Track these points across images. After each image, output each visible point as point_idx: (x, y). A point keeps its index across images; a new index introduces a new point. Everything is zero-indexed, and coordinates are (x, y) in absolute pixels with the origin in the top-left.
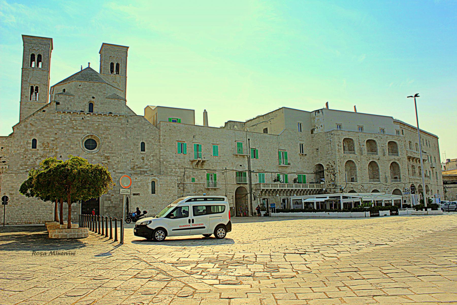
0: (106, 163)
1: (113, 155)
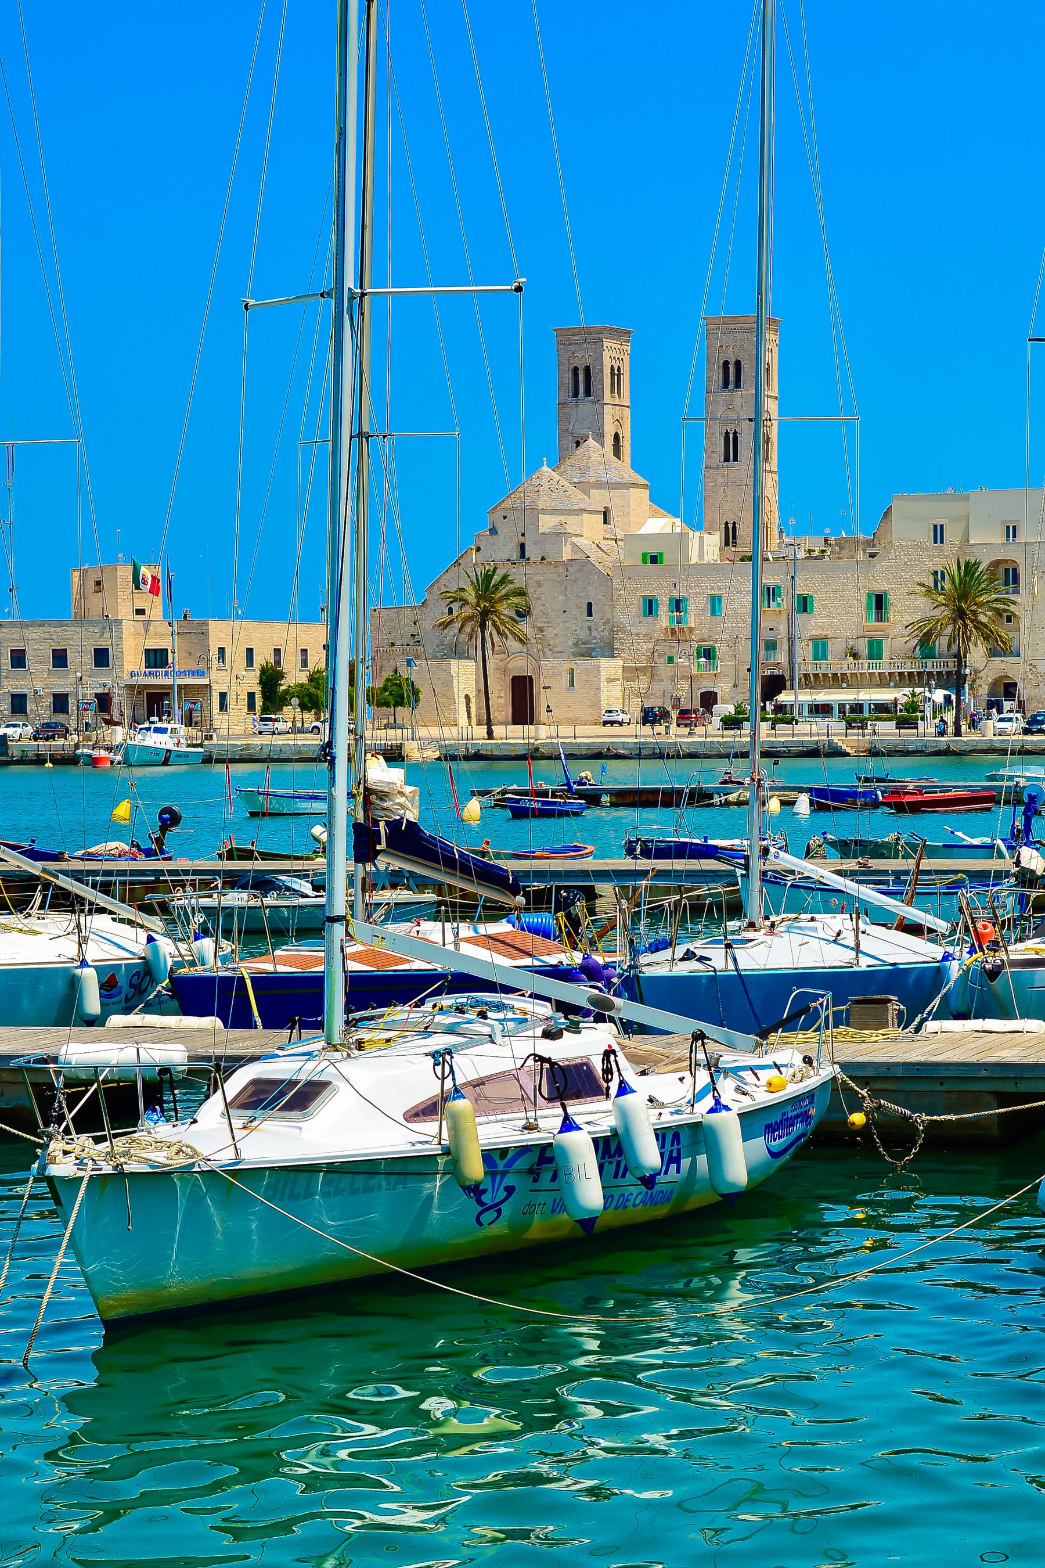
0: (540, 638)
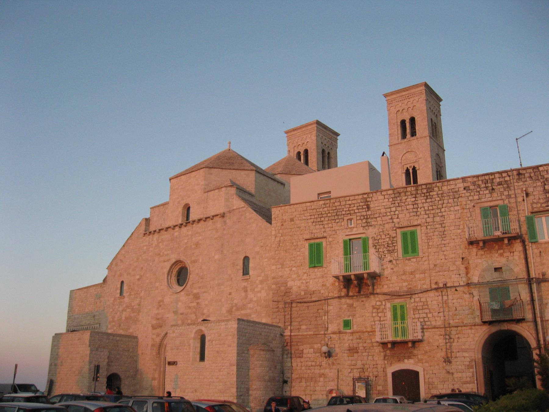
0: (194, 307)
1: (203, 290)
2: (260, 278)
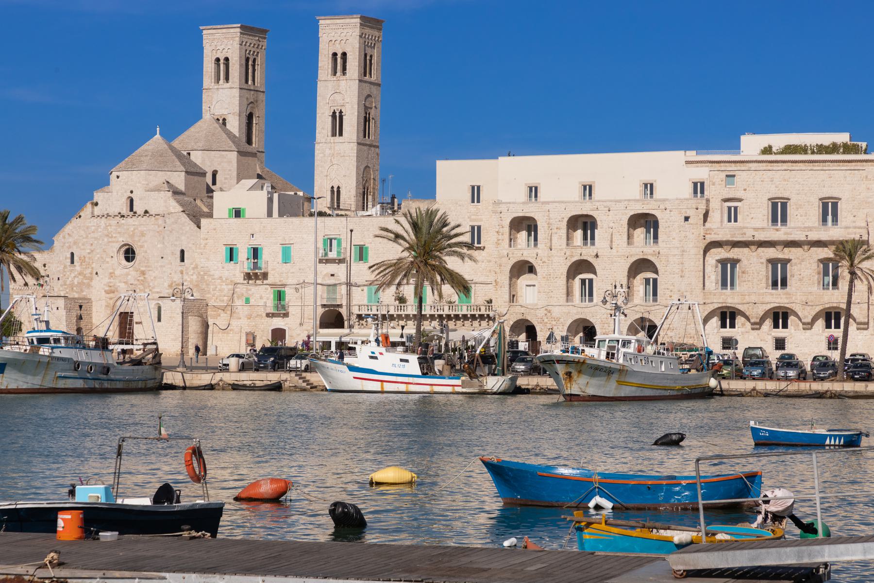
0: (142, 280)
2: (193, 266)
